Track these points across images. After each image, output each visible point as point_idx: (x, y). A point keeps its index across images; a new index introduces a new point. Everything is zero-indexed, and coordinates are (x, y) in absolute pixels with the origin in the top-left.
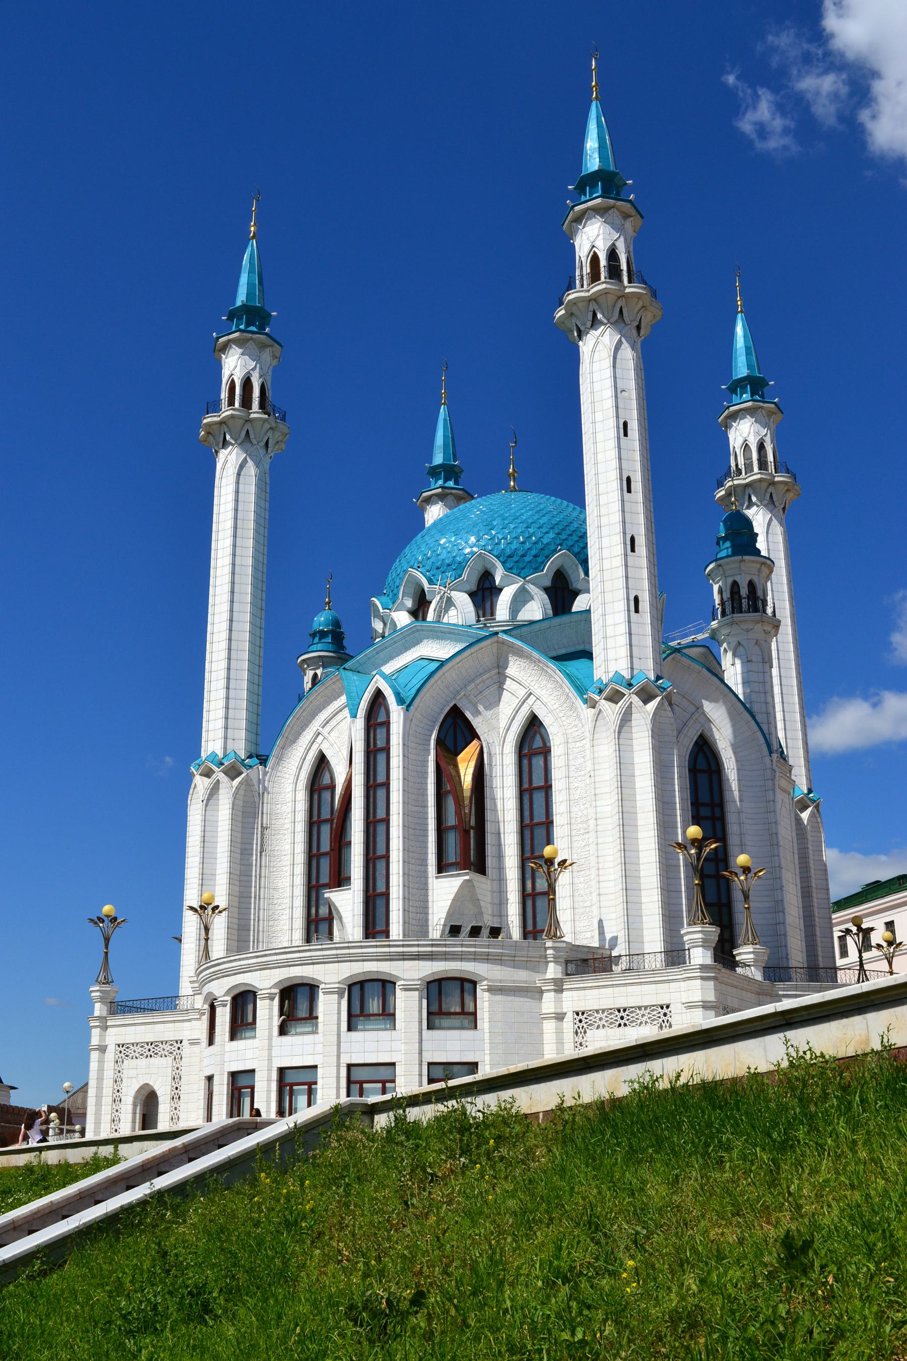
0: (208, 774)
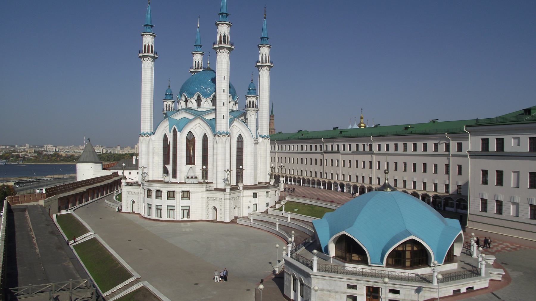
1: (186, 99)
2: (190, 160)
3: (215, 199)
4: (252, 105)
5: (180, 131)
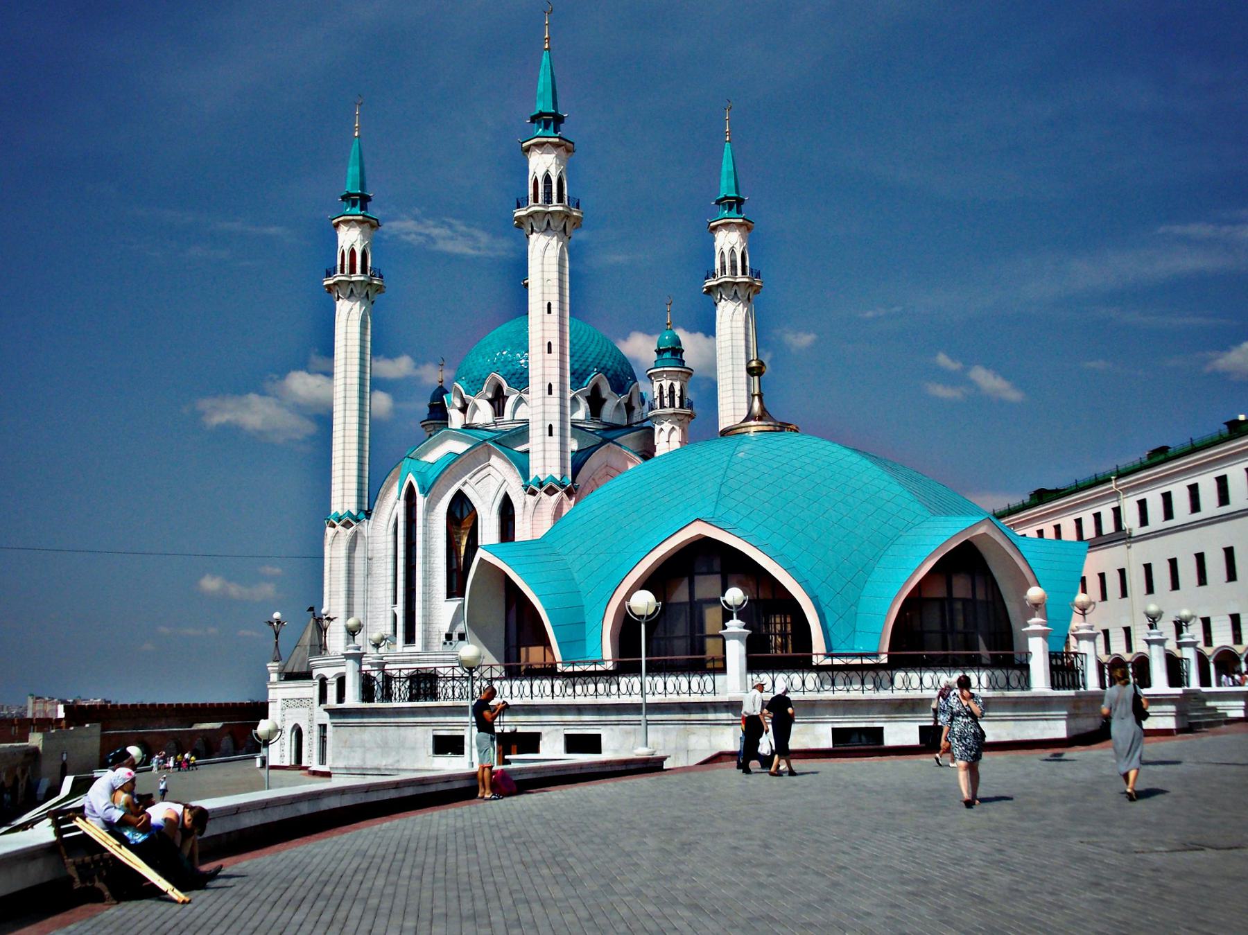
0: (334, 526)
1: (463, 400)
4: (667, 402)
5: (425, 491)
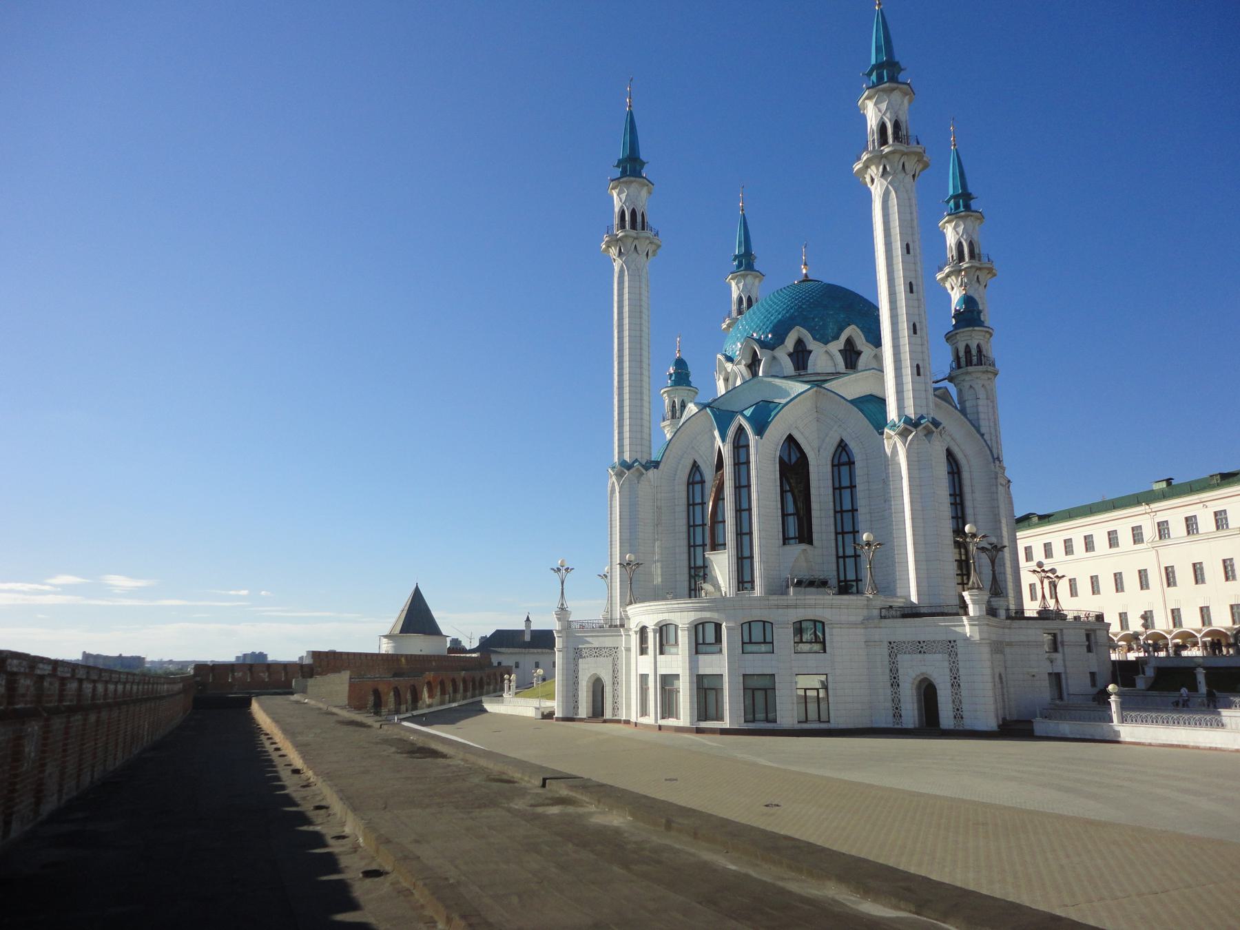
2: (798, 527)
3: (921, 647)
4: (975, 359)
5: (760, 431)
